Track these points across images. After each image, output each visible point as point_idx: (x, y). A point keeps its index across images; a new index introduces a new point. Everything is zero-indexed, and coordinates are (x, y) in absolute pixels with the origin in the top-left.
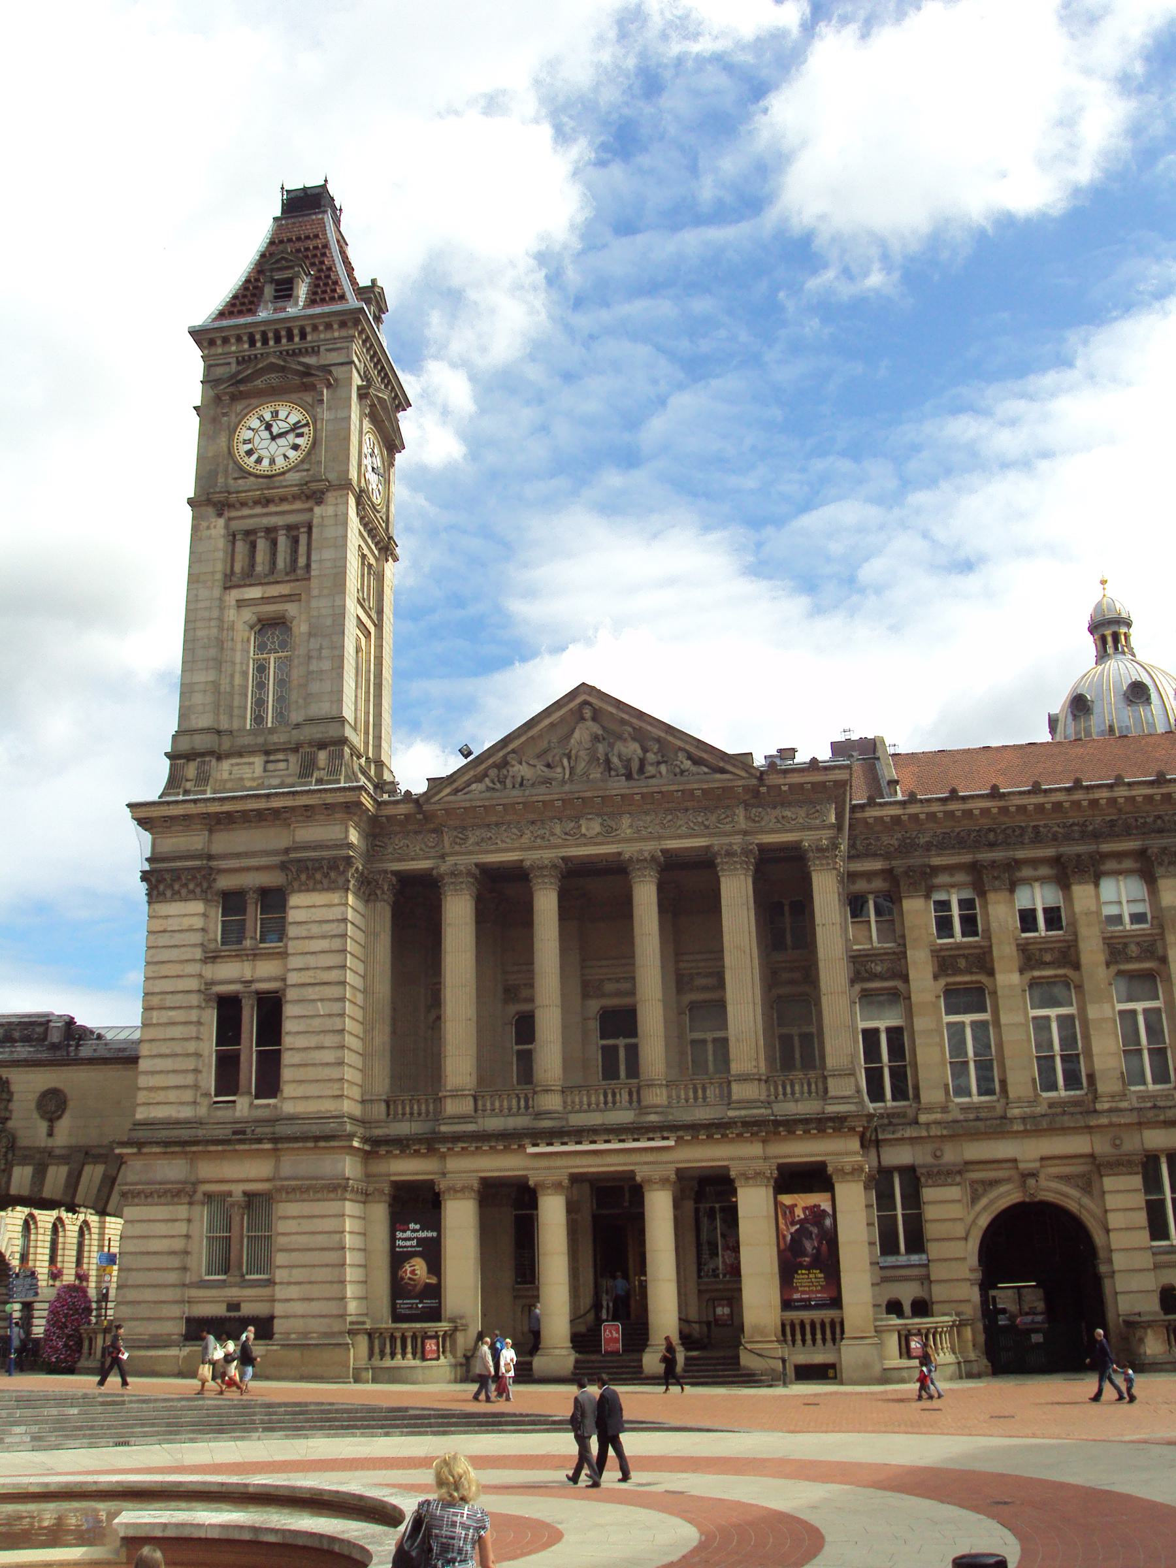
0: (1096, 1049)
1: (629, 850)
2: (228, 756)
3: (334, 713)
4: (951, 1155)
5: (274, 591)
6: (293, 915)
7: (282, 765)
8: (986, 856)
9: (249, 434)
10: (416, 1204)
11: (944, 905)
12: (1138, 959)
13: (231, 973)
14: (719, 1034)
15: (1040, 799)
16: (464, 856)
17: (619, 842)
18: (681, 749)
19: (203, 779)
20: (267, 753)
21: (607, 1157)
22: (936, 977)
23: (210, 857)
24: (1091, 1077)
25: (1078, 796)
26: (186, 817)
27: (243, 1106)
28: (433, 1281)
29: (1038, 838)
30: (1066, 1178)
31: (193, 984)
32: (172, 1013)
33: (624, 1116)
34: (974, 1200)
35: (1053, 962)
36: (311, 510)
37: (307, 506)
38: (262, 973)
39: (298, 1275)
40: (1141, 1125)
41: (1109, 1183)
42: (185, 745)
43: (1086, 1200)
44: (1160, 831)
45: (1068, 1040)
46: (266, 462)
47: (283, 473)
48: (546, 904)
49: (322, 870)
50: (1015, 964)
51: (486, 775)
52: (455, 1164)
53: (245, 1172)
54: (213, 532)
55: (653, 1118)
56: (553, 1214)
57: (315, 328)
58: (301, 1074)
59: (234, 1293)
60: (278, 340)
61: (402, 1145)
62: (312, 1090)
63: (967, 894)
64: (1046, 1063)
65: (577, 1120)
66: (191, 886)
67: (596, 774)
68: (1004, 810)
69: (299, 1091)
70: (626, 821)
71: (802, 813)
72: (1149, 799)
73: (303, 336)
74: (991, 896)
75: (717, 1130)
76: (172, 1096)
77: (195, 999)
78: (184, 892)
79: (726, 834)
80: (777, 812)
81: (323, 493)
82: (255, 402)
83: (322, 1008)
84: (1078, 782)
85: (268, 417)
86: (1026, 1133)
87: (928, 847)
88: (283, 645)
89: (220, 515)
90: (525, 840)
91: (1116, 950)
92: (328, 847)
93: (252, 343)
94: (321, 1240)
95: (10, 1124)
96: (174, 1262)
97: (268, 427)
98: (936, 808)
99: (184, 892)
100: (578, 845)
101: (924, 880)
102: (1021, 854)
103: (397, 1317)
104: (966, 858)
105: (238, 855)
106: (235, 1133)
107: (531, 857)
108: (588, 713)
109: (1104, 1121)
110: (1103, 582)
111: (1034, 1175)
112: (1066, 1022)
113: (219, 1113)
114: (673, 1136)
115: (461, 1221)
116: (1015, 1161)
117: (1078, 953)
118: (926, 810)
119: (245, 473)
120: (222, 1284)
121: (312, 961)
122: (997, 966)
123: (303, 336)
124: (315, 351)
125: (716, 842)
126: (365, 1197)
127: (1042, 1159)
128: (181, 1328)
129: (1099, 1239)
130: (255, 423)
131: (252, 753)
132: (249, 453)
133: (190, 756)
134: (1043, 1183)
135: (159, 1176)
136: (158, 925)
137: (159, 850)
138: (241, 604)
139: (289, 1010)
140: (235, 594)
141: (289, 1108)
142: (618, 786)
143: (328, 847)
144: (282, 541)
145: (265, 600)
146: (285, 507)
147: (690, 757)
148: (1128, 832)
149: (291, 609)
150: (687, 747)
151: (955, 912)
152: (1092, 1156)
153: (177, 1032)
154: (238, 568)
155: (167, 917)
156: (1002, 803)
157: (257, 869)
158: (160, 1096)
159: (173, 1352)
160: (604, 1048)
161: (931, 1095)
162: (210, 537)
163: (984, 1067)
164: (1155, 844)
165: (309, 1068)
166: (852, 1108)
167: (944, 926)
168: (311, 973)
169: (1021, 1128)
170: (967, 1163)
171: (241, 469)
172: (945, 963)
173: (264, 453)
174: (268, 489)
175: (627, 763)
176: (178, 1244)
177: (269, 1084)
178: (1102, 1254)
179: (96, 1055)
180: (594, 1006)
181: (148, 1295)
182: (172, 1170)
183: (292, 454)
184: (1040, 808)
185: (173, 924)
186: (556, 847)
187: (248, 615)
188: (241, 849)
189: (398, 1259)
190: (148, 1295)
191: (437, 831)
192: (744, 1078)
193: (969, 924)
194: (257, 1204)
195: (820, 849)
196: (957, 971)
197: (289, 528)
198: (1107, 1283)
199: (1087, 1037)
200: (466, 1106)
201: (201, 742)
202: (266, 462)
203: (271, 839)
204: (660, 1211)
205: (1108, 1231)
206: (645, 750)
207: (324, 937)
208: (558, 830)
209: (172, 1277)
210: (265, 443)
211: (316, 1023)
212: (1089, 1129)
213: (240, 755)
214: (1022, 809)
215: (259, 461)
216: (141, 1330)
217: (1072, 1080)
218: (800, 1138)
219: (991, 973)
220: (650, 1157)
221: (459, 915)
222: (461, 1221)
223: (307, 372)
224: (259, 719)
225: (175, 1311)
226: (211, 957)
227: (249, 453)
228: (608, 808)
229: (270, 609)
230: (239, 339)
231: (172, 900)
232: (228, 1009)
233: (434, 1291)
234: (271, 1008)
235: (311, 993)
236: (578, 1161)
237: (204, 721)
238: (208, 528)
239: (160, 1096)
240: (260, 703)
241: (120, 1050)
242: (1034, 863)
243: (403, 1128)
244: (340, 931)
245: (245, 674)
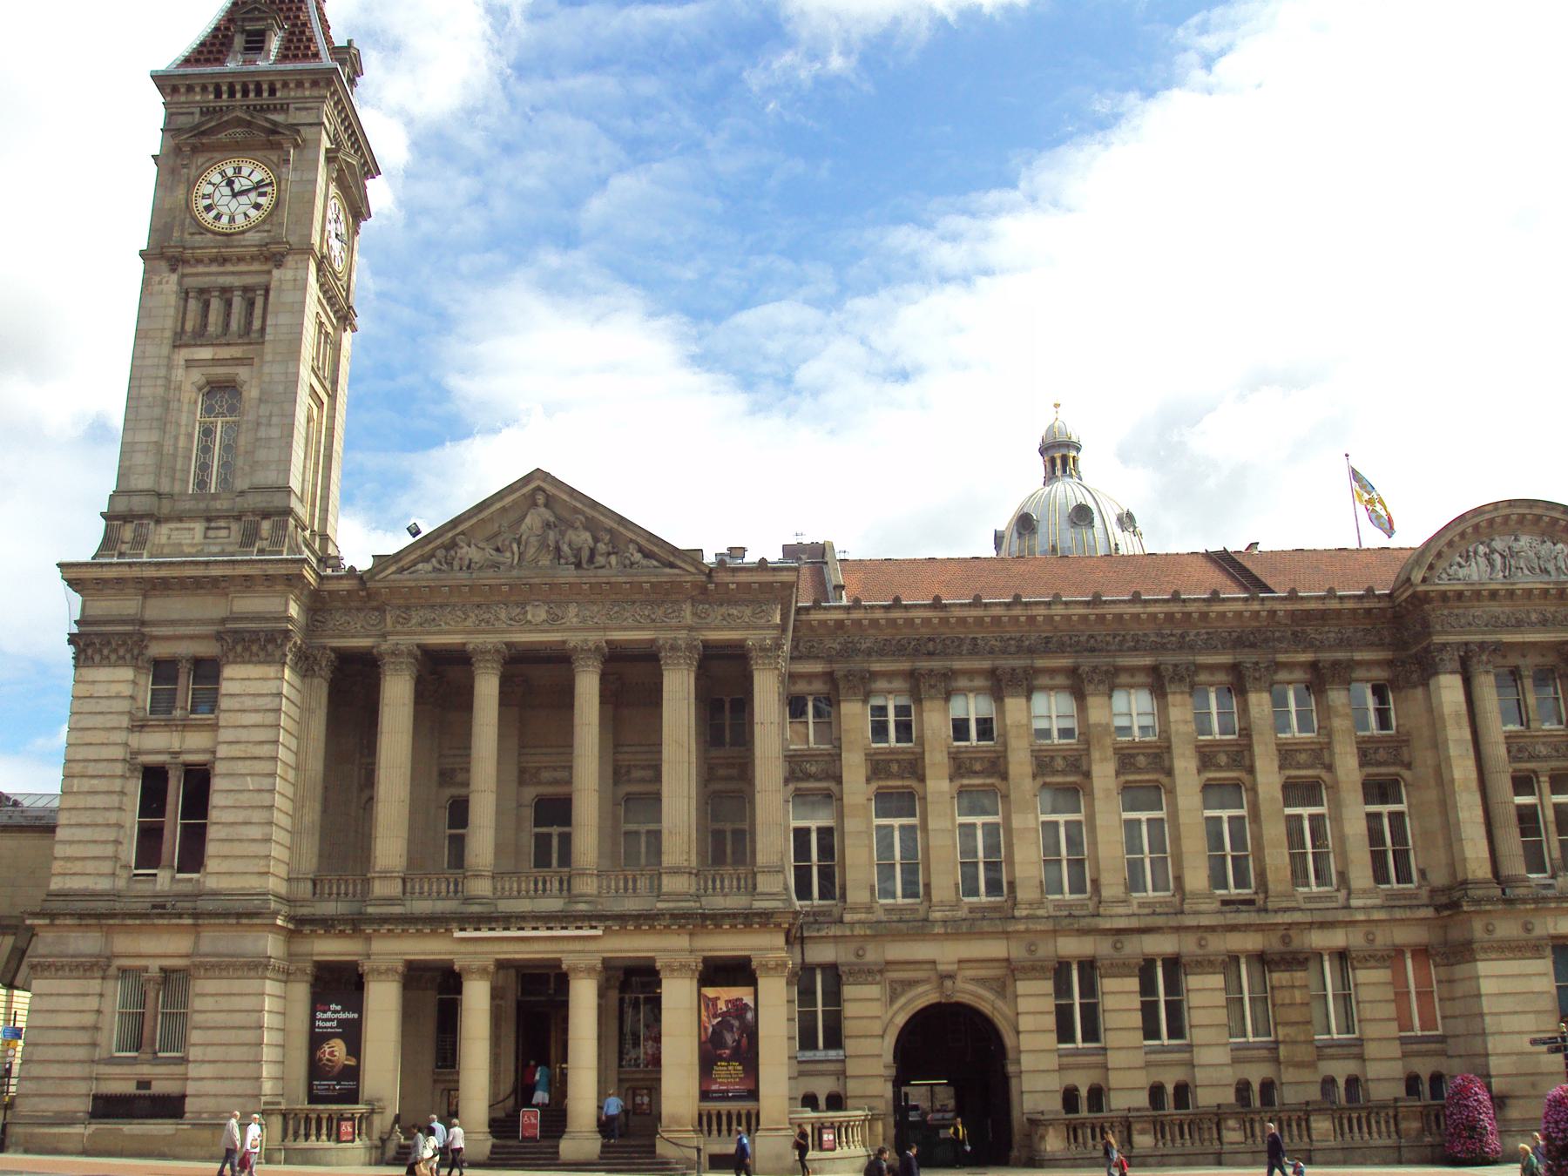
0: (1018, 858)
1: (574, 639)
2: (168, 519)
3: (281, 483)
4: (872, 955)
5: (225, 353)
6: (226, 687)
7: (223, 533)
8: (924, 664)
9: (209, 189)
10: (339, 985)
11: (882, 710)
12: (1063, 773)
13: (158, 744)
14: (652, 827)
15: (979, 612)
17: (564, 630)
18: (631, 541)
19: (140, 542)
20: (209, 519)
21: (532, 945)
22: (868, 780)
23: (143, 623)
24: (1011, 884)
25: (1017, 611)
26: (119, 581)
27: (164, 880)
28: (352, 1062)
29: (975, 650)
30: (981, 981)
31: (119, 753)
32: (95, 782)
33: (553, 904)
34: (892, 1000)
35: (982, 773)
36: (269, 272)
37: (265, 268)
38: (193, 745)
39: (212, 1053)
40: (1055, 932)
41: (1022, 987)
42: (122, 506)
43: (999, 1003)
44: (1092, 650)
45: (992, 848)
46: (225, 219)
47: (243, 232)
48: (487, 688)
49: (259, 642)
50: (946, 771)
51: (433, 556)
52: (378, 946)
53: (161, 948)
54: (165, 287)
55: (582, 907)
56: (477, 999)
57: (285, 85)
58: (225, 849)
59: (145, 1070)
60: (245, 93)
61: (327, 925)
62: (238, 866)
63: (903, 701)
64: (969, 868)
65: (506, 906)
66: (122, 652)
67: (545, 561)
68: (944, 621)
69: (225, 866)
70: (572, 610)
71: (748, 612)
72: (1084, 618)
73: (272, 92)
74: (927, 705)
75: (644, 921)
76: (90, 867)
77: (119, 769)
78: (113, 657)
79: (671, 629)
80: (723, 610)
81: (283, 256)
82: (217, 155)
83: (250, 783)
84: (1017, 597)
85: (230, 172)
86: (947, 936)
87: (869, 653)
88: (232, 410)
89: (173, 270)
90: (469, 623)
91: (1043, 763)
92: (267, 620)
93: (218, 94)
94: (238, 1019)
96: (84, 1037)
97: (230, 183)
98: (879, 614)
99: (113, 657)
100: (521, 632)
101: (863, 685)
102: (957, 665)
103: (313, 1099)
104: (905, 666)
105: (173, 623)
106: (154, 907)
107: (474, 641)
108: (541, 499)
109: (1021, 927)
111: (951, 976)
112: (991, 830)
113: (139, 886)
114: (601, 927)
115: (383, 1005)
116: (934, 962)
117: (1006, 763)
118: (870, 616)
119: (203, 230)
120: (133, 1062)
121: (243, 735)
122: (928, 772)
123: (272, 92)
124: (284, 108)
125: (663, 636)
126: (287, 976)
127: (960, 962)
128: (85, 1105)
129: (1009, 1040)
130: (216, 178)
131: (193, 518)
132: (208, 208)
133: (126, 518)
134: (960, 984)
135: (71, 949)
136: (84, 690)
137: (90, 612)
138: (190, 364)
139: (217, 784)
140: (184, 354)
141: (212, 883)
142: (568, 574)
143: (267, 620)
144: (237, 302)
145: (215, 362)
146: (242, 267)
147: (640, 550)
148: (1061, 649)
149: (243, 373)
150: (639, 540)
151: (892, 717)
152: (1008, 960)
153: (98, 801)
154: (189, 326)
155: (94, 682)
156: (942, 614)
157: (192, 637)
158: (78, 867)
159: (78, 1129)
160: (537, 836)
161: (857, 895)
162: (162, 292)
163: (910, 871)
164: (1087, 662)
165: (236, 844)
166: (780, 904)
167: (880, 730)
168: (242, 747)
169: (942, 931)
170: (888, 963)
171: (198, 224)
172: (878, 767)
173: (223, 209)
174: (226, 250)
175: (577, 552)
176: (89, 1019)
177: (193, 857)
178: (1011, 1055)
179: (10, 822)
180: (530, 793)
181: (54, 1071)
182: (86, 943)
183: (253, 213)
184: (979, 621)
185: (100, 690)
186: (503, 632)
187: (197, 376)
188: (175, 616)
189: (316, 1040)
190: (54, 1071)
191: (381, 609)
192: (675, 871)
193: (904, 730)
194: (174, 980)
195: (763, 649)
196: (890, 776)
197: (246, 289)
198: (1014, 1082)
199: (1010, 846)
200: (395, 888)
201: (140, 504)
202: (225, 219)
203: (209, 608)
204: (584, 999)
205: (1018, 1033)
206: (596, 540)
207: (256, 711)
208: (503, 615)
209: (81, 1053)
210: (225, 200)
212: (1006, 935)
213: (180, 520)
214: (962, 621)
215: (218, 217)
216: (43, 1107)
217: (994, 887)
218: (726, 932)
219: (922, 779)
220: (578, 946)
221: (397, 696)
222: (383, 1005)
223: (274, 130)
224: (202, 484)
225: (82, 1088)
226: (139, 726)
227: (208, 208)
228: (556, 596)
229: (221, 371)
230: (204, 89)
231: (100, 665)
232: (153, 779)
233: (353, 1073)
234: (199, 781)
235: (241, 767)
236: (506, 947)
237: (145, 482)
238: (160, 283)
239: (78, 867)
240: (204, 467)
241: (37, 818)
242: (970, 674)
243: (329, 908)
244: (274, 705)
245: (190, 436)
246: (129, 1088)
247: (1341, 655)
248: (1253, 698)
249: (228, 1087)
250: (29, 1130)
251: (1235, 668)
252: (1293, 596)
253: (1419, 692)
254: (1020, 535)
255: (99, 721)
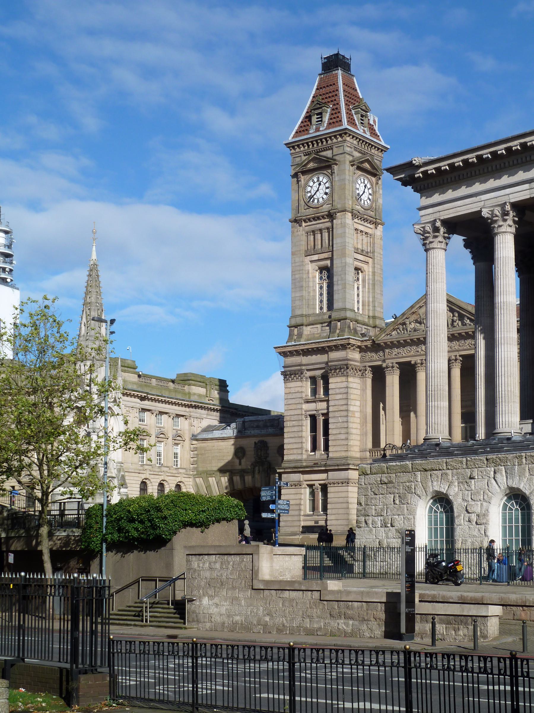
3: (343, 307)
19: (300, 335)
42: (293, 322)
54: (299, 233)
83: (340, 420)
94: (341, 500)
95: (268, 459)
105: (313, 364)
106: (314, 464)
136: (288, 391)
137: (287, 363)
138: (312, 262)
158: (291, 452)
159: (297, 537)
165: (338, 441)
168: (336, 407)
185: (293, 390)
187: (315, 266)
188: (313, 362)
201: (298, 321)
211: (339, 425)
213: (313, 325)
216: (287, 530)
223: (327, 160)
232: (313, 418)
238: (297, 232)
244: (345, 391)
245: (314, 291)
246: (312, 523)
249: (339, 522)
250: (284, 537)
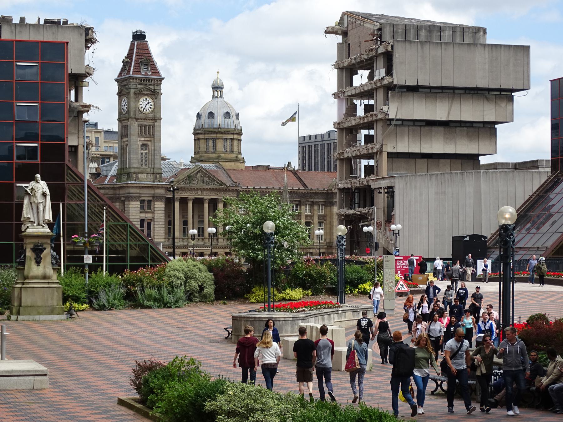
1: (205, 197)
9: (141, 103)
13: (143, 216)
16: (178, 196)
38: (149, 216)
48: (190, 205)
49: (159, 199)
62: (159, 237)
67: (202, 183)
73: (152, 81)
77: (139, 220)
107: (189, 197)
110: (218, 73)
121: (159, 215)
124: (154, 85)
140: (139, 139)
146: (148, 121)
149: (149, 143)
175: (207, 182)
180: (183, 220)
187: (140, 143)
228: (203, 190)
229: (145, 142)
235: (159, 220)
247: (317, 200)
248: (302, 207)
251: (300, 201)
252: (312, 189)
253: (329, 207)
254: (209, 118)
255: (134, 212)
